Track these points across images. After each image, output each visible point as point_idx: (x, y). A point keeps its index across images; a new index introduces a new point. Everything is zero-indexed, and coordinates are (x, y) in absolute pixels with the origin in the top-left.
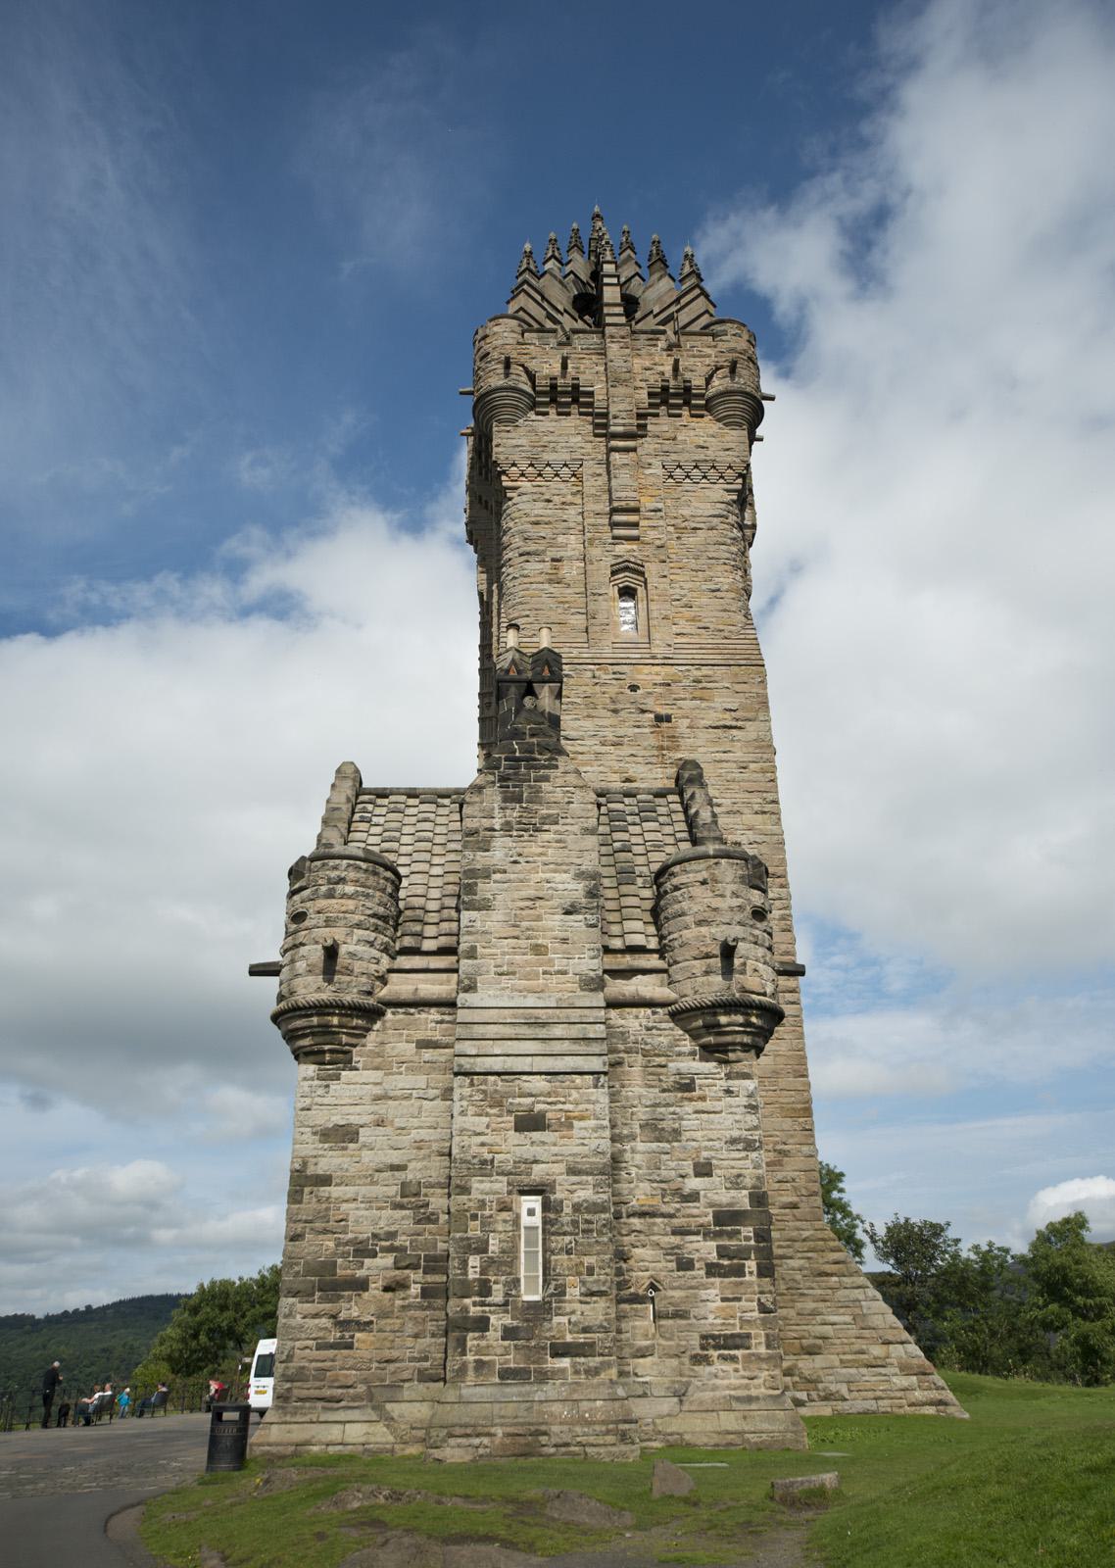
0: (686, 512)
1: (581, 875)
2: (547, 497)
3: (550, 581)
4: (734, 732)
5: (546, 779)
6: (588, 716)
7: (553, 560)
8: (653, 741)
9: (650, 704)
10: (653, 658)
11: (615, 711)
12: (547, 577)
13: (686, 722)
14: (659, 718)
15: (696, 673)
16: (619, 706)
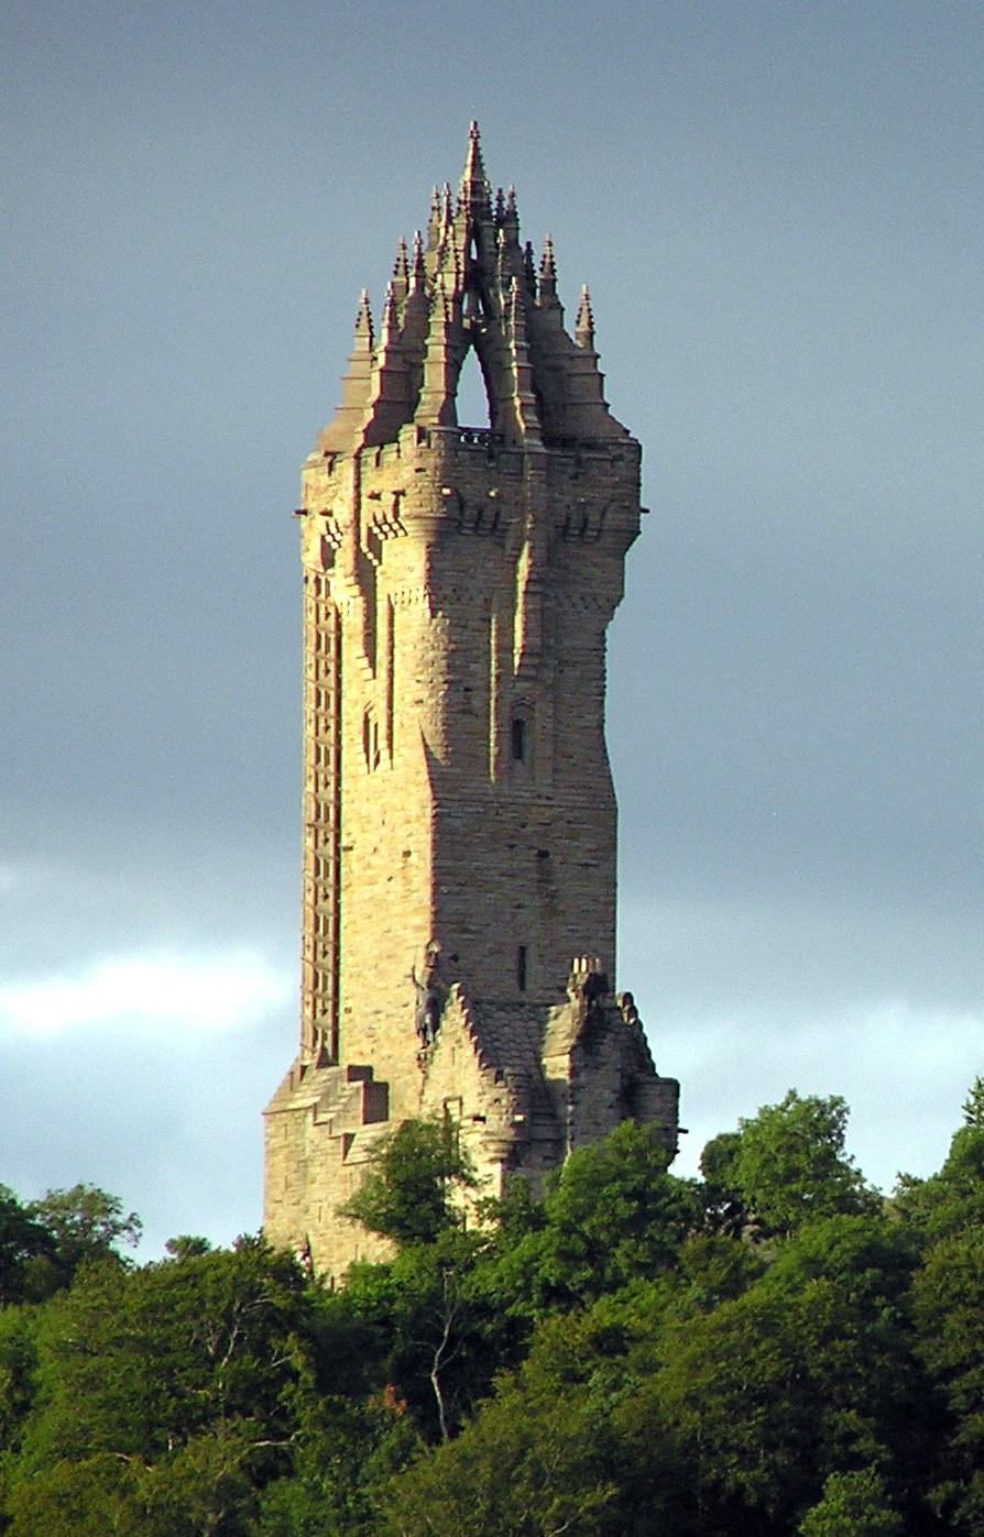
0: (567, 643)
1: (615, 1092)
2: (463, 623)
3: (463, 712)
4: (592, 869)
5: (602, 1044)
6: (494, 850)
7: (467, 690)
8: (536, 876)
9: (535, 841)
10: (539, 797)
11: (512, 847)
12: (461, 707)
13: (559, 858)
14: (543, 854)
15: (571, 816)
16: (514, 842)
